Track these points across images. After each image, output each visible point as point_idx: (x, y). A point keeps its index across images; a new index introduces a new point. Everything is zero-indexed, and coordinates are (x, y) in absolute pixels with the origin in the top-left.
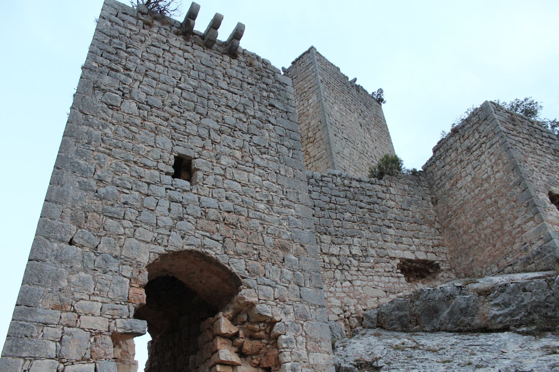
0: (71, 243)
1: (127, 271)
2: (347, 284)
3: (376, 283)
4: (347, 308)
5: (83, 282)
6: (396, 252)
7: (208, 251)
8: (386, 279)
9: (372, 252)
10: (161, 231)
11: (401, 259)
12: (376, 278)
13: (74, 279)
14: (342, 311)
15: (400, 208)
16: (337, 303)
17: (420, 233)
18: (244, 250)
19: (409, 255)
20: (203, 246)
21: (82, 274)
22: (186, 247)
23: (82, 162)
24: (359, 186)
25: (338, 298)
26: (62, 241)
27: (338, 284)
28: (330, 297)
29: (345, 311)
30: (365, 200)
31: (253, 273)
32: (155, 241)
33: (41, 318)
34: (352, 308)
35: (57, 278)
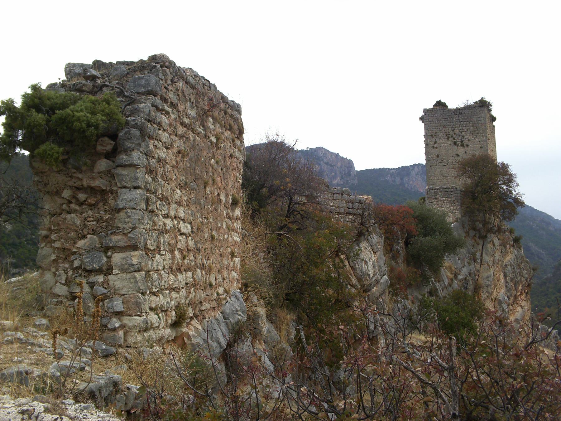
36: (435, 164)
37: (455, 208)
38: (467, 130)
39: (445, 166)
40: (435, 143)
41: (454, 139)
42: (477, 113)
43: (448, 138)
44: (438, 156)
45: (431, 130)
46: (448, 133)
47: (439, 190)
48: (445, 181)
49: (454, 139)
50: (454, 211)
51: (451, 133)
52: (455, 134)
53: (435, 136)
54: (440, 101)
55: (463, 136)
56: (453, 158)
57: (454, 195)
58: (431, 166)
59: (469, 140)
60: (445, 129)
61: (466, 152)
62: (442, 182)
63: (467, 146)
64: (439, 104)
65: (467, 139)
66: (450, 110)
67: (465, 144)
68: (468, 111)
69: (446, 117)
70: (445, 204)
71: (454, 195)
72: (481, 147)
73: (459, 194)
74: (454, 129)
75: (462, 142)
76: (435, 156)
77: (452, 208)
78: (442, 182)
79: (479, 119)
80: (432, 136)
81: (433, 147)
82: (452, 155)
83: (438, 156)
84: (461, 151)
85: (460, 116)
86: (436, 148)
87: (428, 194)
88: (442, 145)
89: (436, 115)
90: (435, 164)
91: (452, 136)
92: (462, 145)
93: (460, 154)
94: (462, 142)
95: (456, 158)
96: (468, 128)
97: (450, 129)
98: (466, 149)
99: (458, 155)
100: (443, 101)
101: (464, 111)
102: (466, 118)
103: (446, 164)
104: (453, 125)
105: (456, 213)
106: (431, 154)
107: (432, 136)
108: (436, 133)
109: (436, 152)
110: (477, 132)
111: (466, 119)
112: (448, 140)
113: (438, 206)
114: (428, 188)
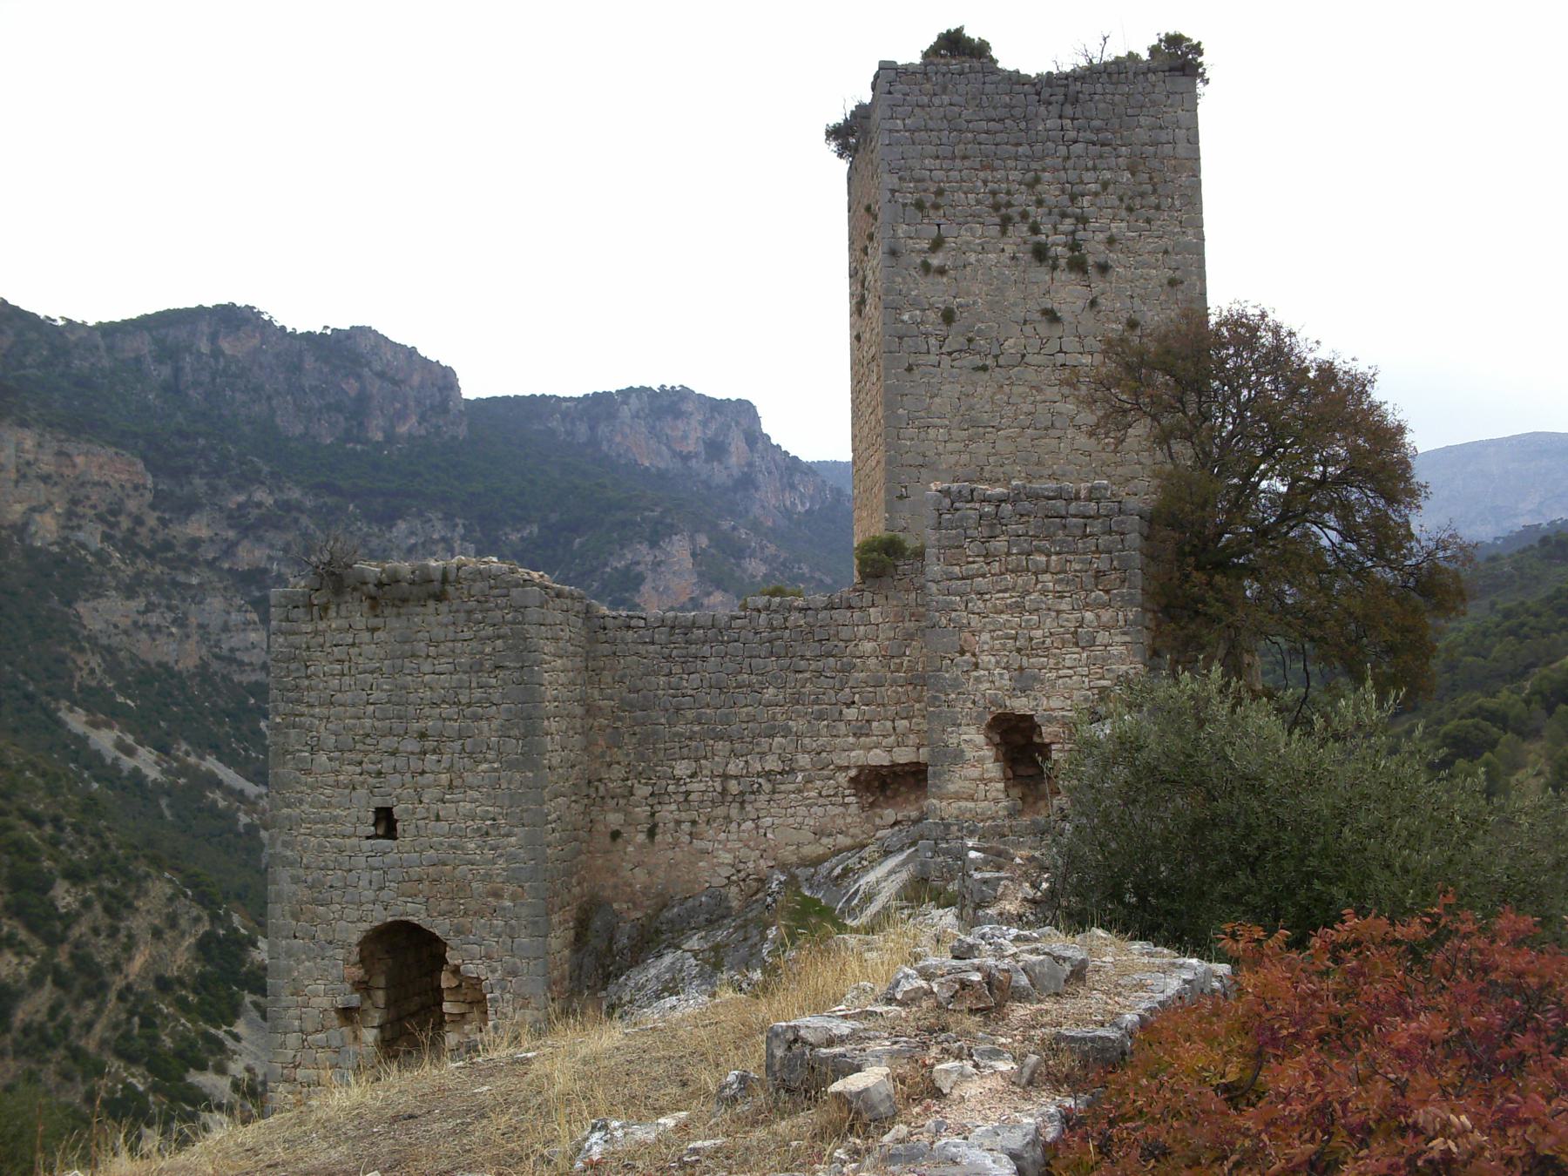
0: (295, 937)
1: (340, 954)
2: (749, 824)
3: (799, 819)
4: (741, 866)
5: (309, 970)
6: (853, 754)
7: (410, 918)
8: (820, 811)
9: (804, 760)
10: (364, 907)
11: (861, 768)
12: (802, 810)
13: (301, 968)
14: (734, 871)
15: (883, 656)
16: (727, 858)
17: (917, 706)
18: (448, 908)
19: (878, 758)
20: (407, 914)
21: (307, 964)
22: (389, 919)
23: (289, 853)
24: (802, 622)
25: (730, 851)
26: (287, 937)
27: (734, 826)
28: (718, 849)
29: (739, 871)
30: (808, 654)
31: (459, 931)
32: (360, 920)
33: (284, 1004)
34: (751, 865)
35: (289, 970)
36: (933, 359)
37: (1106, 615)
38: (1105, 185)
39: (984, 368)
40: (937, 244)
41: (1035, 230)
42: (1154, 103)
43: (1006, 222)
44: (948, 316)
45: (917, 173)
46: (1002, 198)
47: (1007, 508)
48: (982, 448)
49: (1035, 230)
50: (1102, 637)
51: (1022, 198)
52: (1040, 203)
53: (936, 207)
54: (959, 31)
55: (1082, 220)
56: (1028, 329)
57: (1103, 540)
58: (910, 369)
59: (1111, 241)
60: (988, 174)
61: (1093, 303)
62: (965, 458)
63: (1104, 268)
64: (953, 44)
65: (1101, 236)
66: (1016, 79)
67: (1091, 260)
68: (1110, 88)
69: (993, 114)
70: (1044, 592)
71: (1103, 540)
72: (1173, 283)
73: (1134, 538)
74: (1037, 180)
75: (1074, 246)
76: (932, 316)
77: (1089, 615)
78: (965, 458)
79: (1163, 136)
80: (919, 205)
81: (926, 267)
82: (1020, 313)
83: (948, 316)
84: (1068, 293)
85: (1068, 110)
86: (942, 271)
87: (939, 526)
88: (972, 258)
89: (946, 99)
90: (933, 359)
91: (1024, 216)
92: (1078, 265)
93: (1064, 312)
94: (1074, 246)
95: (1043, 329)
96: (1108, 175)
97: (1015, 175)
98: (1098, 285)
99: (1051, 316)
100: (972, 33)
101: (1087, 88)
102: (1096, 123)
103: (989, 362)
104: (1032, 158)
105: (1114, 650)
106: (915, 304)
107: (919, 205)
108: (940, 192)
109: (938, 292)
110: (1153, 200)
111: (1098, 130)
112: (1004, 232)
113: (998, 599)
114: (946, 493)
